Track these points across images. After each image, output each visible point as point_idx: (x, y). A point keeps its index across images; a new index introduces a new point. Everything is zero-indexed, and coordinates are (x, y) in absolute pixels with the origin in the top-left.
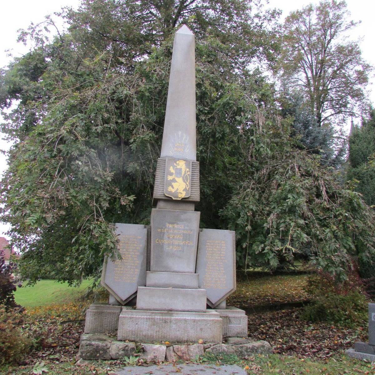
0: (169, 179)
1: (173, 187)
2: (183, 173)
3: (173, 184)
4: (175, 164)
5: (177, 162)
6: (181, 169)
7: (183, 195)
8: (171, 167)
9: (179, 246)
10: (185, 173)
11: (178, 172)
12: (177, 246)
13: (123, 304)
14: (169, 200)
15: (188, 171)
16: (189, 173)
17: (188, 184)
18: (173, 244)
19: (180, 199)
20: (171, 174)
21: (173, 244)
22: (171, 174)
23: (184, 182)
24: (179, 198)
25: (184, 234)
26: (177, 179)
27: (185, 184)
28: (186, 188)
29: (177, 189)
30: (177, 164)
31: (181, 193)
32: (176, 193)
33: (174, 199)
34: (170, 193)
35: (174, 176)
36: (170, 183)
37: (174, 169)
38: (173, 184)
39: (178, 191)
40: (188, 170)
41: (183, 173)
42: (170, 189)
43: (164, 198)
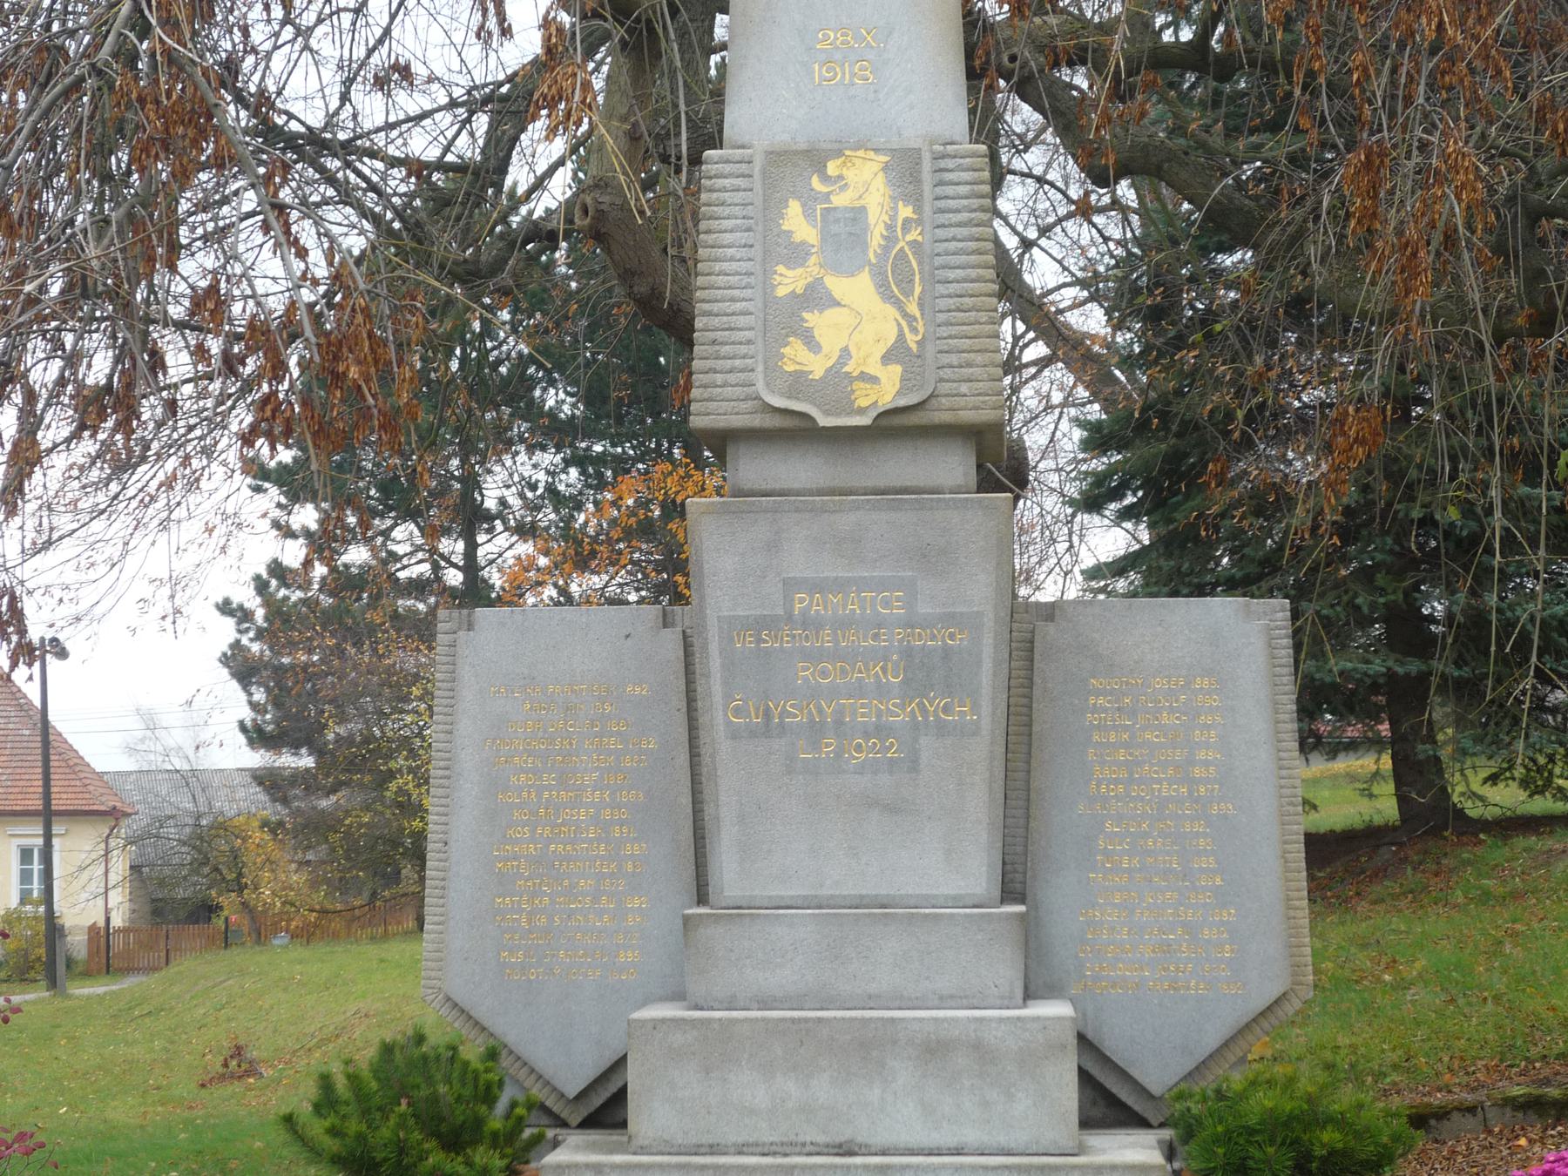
0: (781, 292)
1: (811, 343)
2: (876, 239)
3: (811, 318)
4: (816, 182)
5: (832, 168)
6: (858, 214)
8: (794, 207)
9: (880, 730)
10: (890, 239)
12: (867, 735)
13: (575, 1119)
15: (907, 221)
16: (914, 235)
17: (913, 309)
18: (839, 723)
19: (865, 421)
20: (797, 254)
21: (839, 723)
22: (797, 254)
23: (887, 296)
24: (862, 411)
25: (908, 653)
26: (836, 285)
27: (892, 312)
28: (901, 335)
29: (845, 353)
30: (825, 178)
31: (874, 380)
32: (839, 381)
33: (824, 421)
34: (798, 383)
35: (812, 268)
37: (808, 214)
38: (811, 318)
40: (906, 211)
41: (876, 239)
42: (796, 355)
43: (757, 421)
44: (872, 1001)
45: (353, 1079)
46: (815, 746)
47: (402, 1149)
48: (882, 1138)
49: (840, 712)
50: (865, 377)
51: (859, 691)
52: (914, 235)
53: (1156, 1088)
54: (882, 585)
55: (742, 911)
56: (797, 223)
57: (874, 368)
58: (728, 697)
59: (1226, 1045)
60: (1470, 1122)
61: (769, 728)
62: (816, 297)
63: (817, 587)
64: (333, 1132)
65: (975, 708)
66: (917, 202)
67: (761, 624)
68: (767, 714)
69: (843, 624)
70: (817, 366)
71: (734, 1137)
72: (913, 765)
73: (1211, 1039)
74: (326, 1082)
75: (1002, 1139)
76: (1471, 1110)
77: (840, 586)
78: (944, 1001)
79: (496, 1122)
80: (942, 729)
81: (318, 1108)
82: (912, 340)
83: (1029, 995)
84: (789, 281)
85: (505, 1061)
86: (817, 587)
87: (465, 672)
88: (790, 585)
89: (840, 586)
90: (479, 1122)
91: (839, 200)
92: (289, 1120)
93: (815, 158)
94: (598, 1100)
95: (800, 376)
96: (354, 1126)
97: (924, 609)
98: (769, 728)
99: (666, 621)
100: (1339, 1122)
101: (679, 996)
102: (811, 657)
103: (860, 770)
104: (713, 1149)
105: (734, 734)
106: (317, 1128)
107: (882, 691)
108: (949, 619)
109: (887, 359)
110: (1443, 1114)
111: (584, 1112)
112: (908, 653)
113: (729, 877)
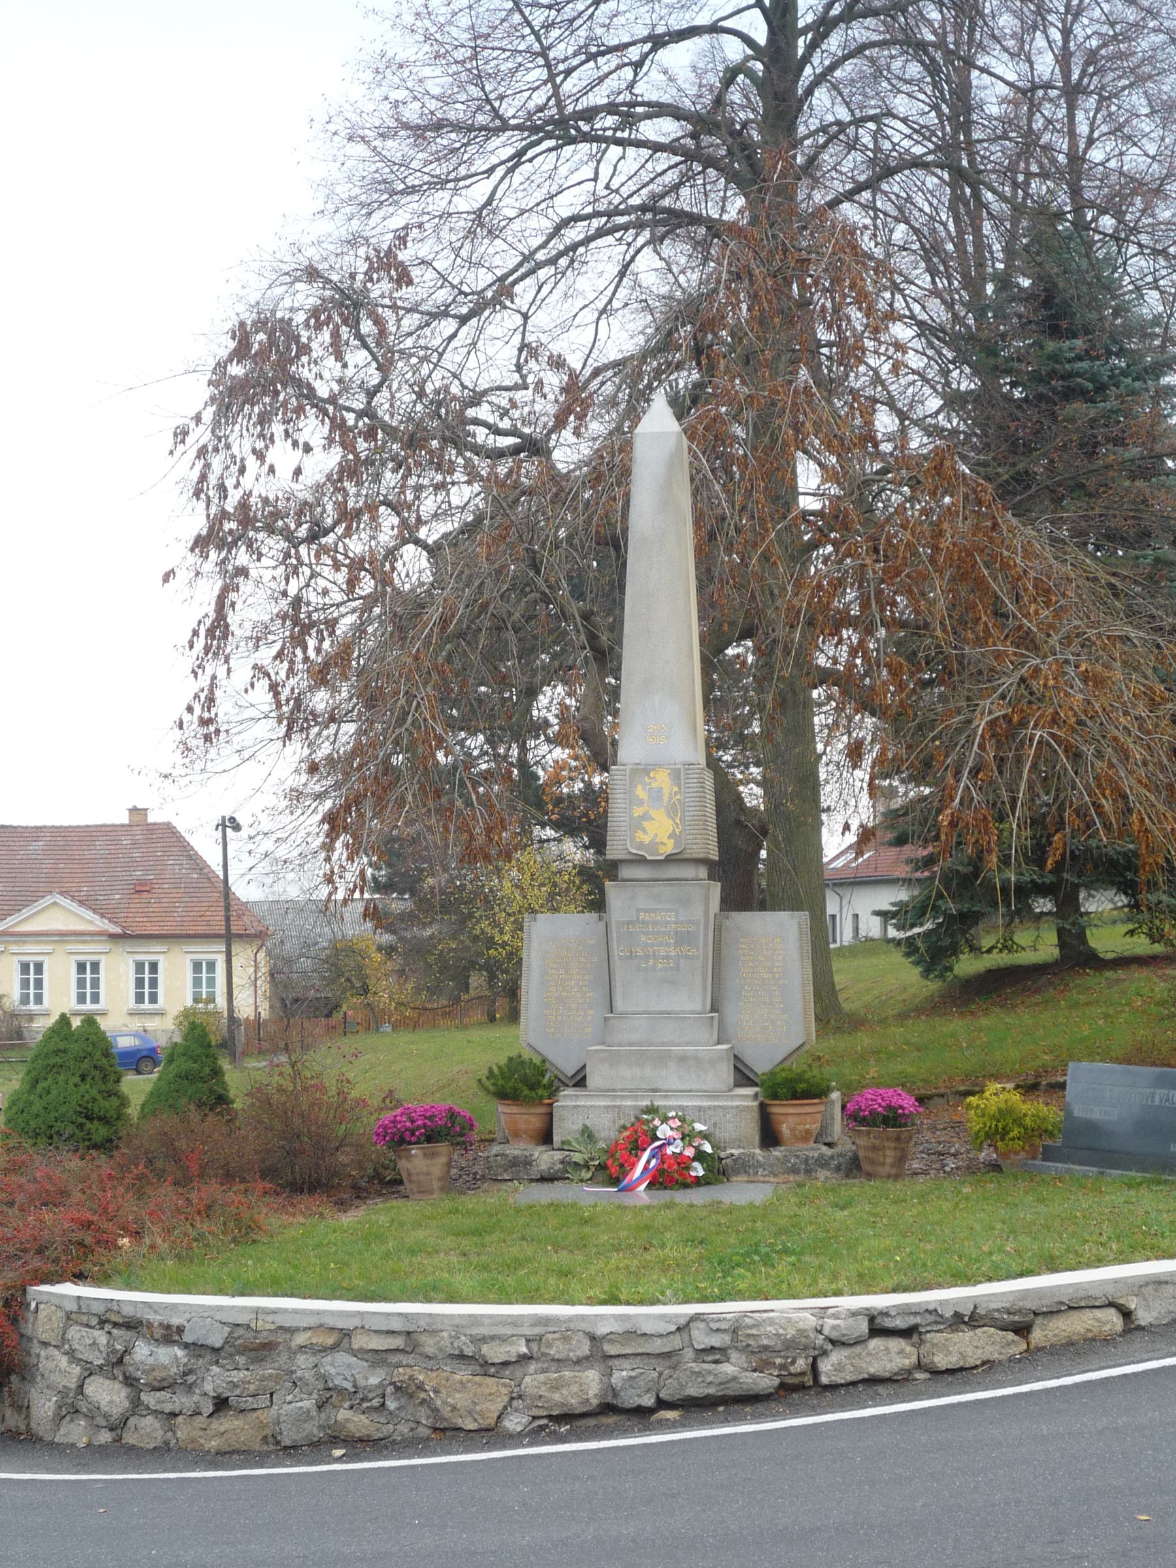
1: (644, 831)
3: (645, 824)
5: (652, 775)
7: (669, 848)
8: (639, 787)
9: (667, 957)
10: (670, 798)
11: (656, 796)
14: (641, 861)
15: (676, 793)
16: (678, 797)
17: (678, 821)
19: (662, 858)
20: (640, 803)
22: (640, 803)
23: (670, 817)
25: (676, 933)
26: (653, 813)
27: (671, 822)
32: (654, 845)
33: (649, 858)
34: (641, 845)
36: (637, 825)
38: (645, 824)
39: (658, 840)
40: (676, 789)
41: (666, 799)
42: (641, 836)
43: (628, 857)
44: (664, 1044)
45: (499, 1067)
46: (647, 962)
47: (516, 1089)
48: (666, 1087)
49: (654, 952)
50: (662, 843)
51: (661, 944)
52: (678, 797)
53: (759, 1072)
54: (670, 910)
55: (624, 1015)
56: (640, 792)
57: (665, 840)
58: (619, 946)
59: (785, 1059)
60: (941, 1100)
61: (632, 956)
62: (646, 817)
63: (646, 911)
64: (494, 1084)
65: (698, 950)
66: (679, 786)
67: (628, 923)
68: (631, 952)
69: (655, 923)
70: (646, 840)
71: (620, 1087)
72: (678, 969)
73: (780, 1059)
74: (491, 1070)
75: (704, 1087)
76: (942, 1096)
77: (654, 911)
78: (687, 1044)
79: (546, 1080)
80: (687, 957)
81: (488, 1078)
82: (677, 831)
83: (718, 1043)
84: (638, 812)
85: (547, 1065)
86: (646, 911)
87: (534, 936)
88: (638, 911)
89: (654, 911)
90: (540, 1082)
91: (654, 785)
92: (480, 1080)
93: (647, 772)
94: (578, 1078)
95: (641, 843)
96: (501, 1082)
97: (681, 918)
98: (632, 956)
99: (600, 919)
100: (807, 1081)
101: (604, 1043)
102: (644, 933)
103: (661, 970)
104: (613, 1091)
105: (621, 958)
106: (487, 1083)
107: (668, 945)
108: (690, 922)
109: (669, 837)
110: (930, 1097)
111: (574, 1081)
112: (676, 933)
113: (620, 1005)
